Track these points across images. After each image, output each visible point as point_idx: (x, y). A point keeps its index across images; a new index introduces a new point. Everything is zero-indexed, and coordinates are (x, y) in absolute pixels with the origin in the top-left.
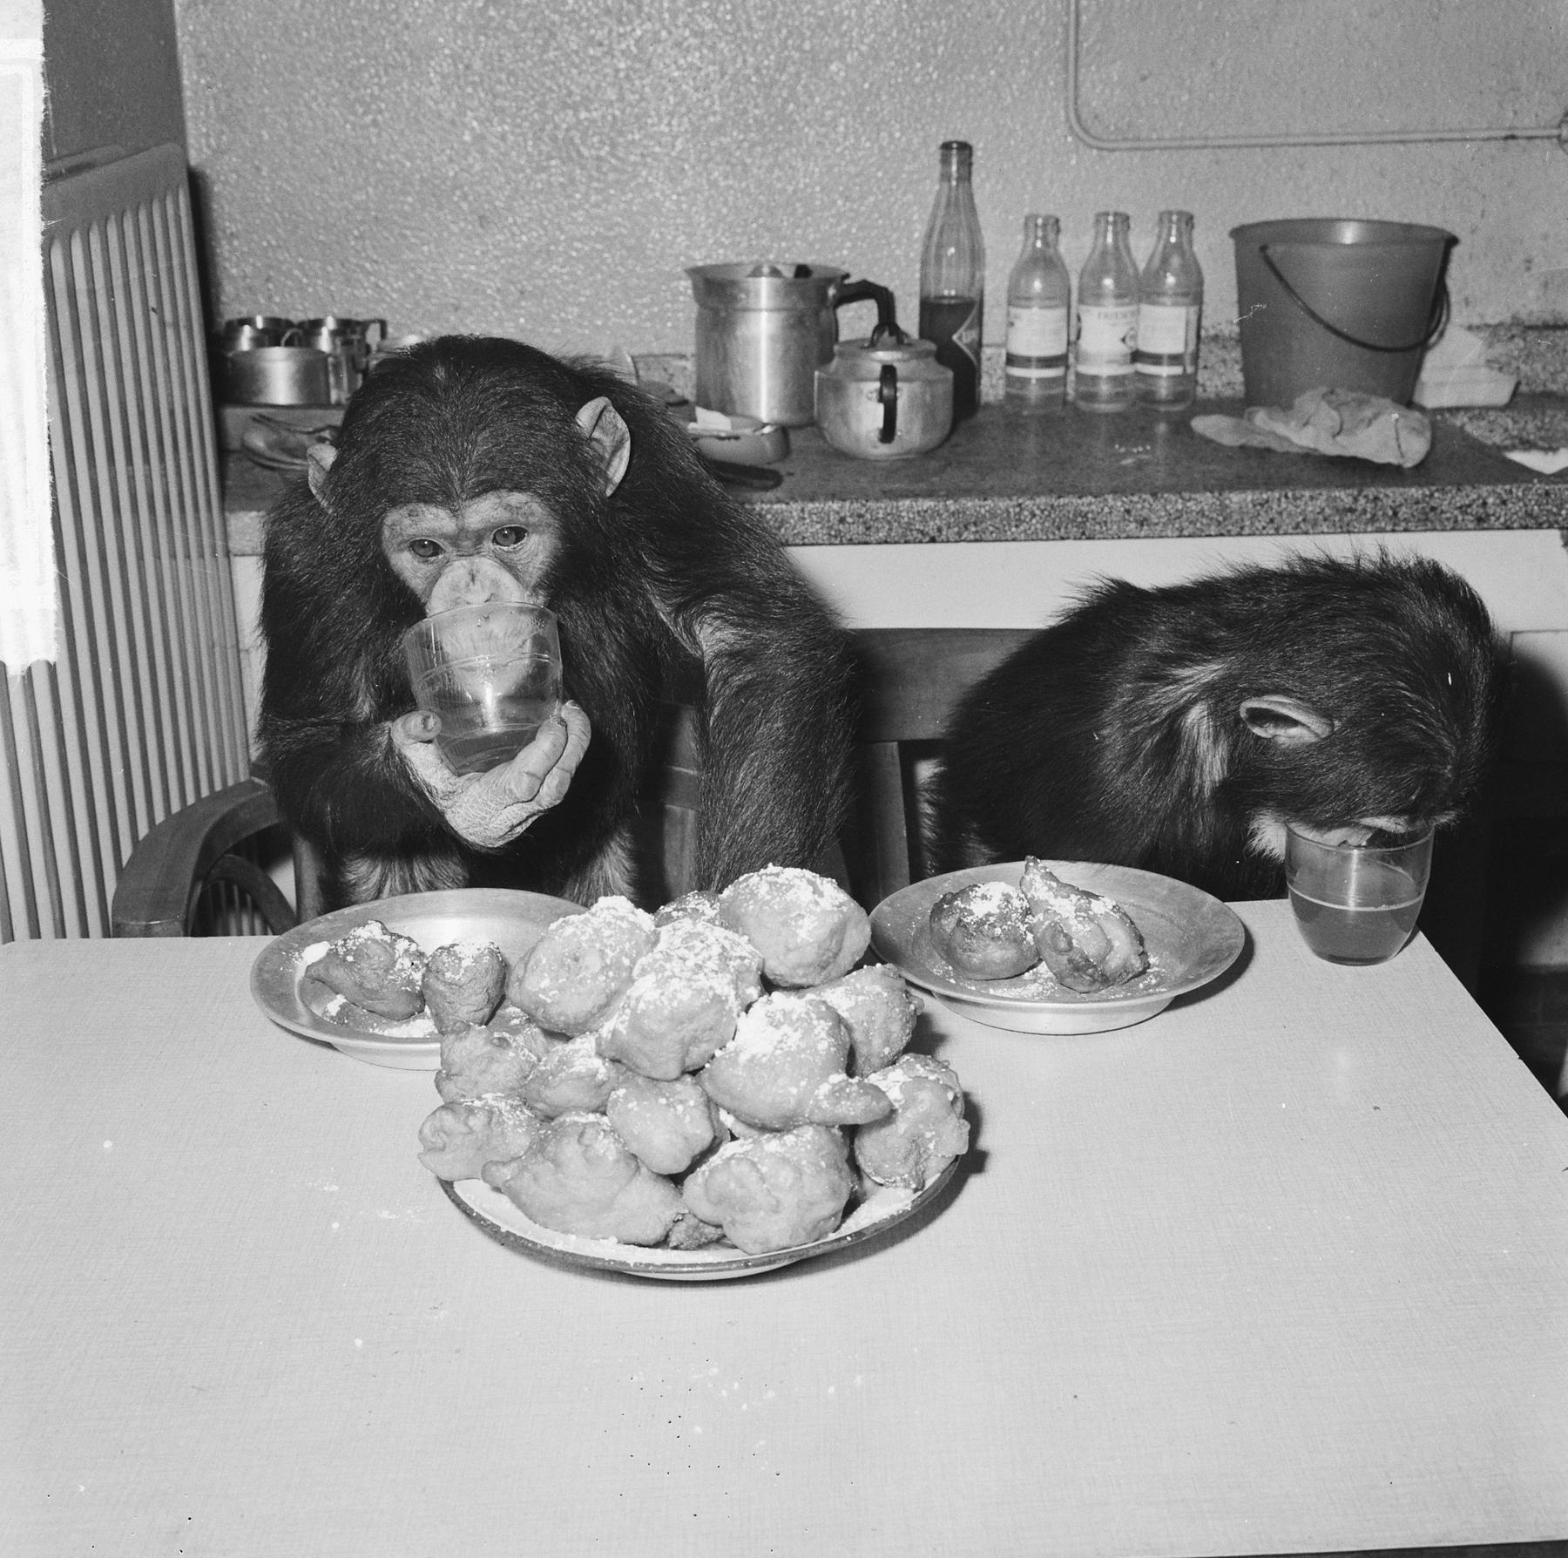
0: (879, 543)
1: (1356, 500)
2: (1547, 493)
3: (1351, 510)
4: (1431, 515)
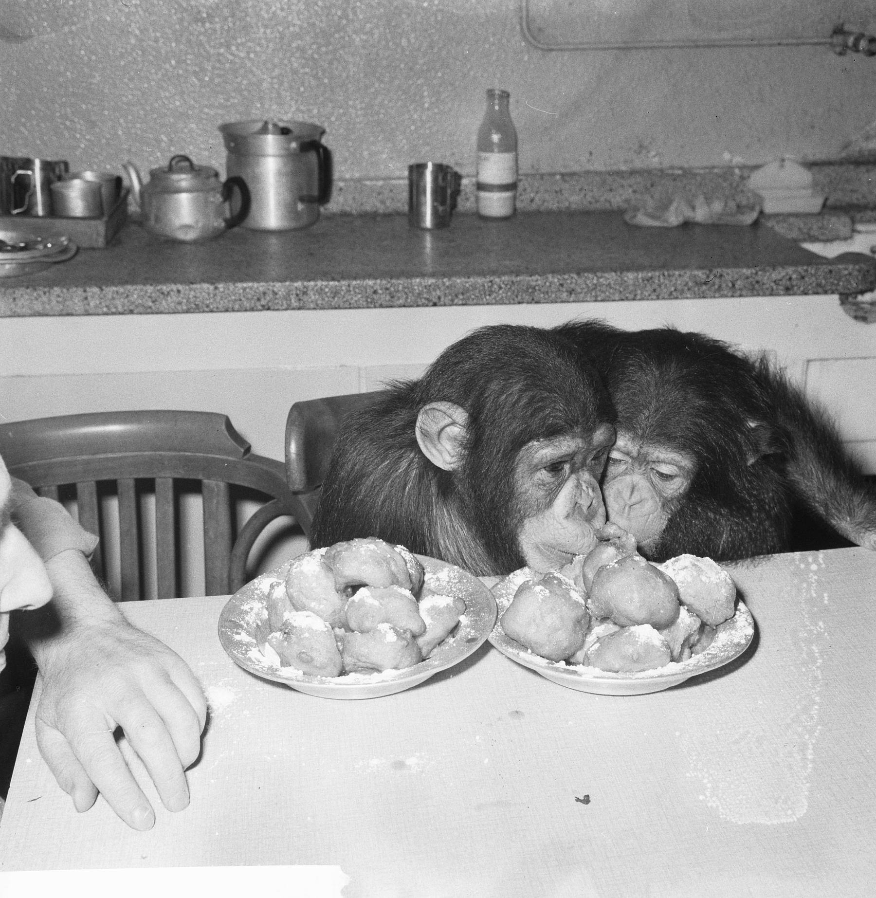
0: (400, 306)
1: (708, 277)
2: (831, 271)
3: (706, 283)
4: (757, 286)
